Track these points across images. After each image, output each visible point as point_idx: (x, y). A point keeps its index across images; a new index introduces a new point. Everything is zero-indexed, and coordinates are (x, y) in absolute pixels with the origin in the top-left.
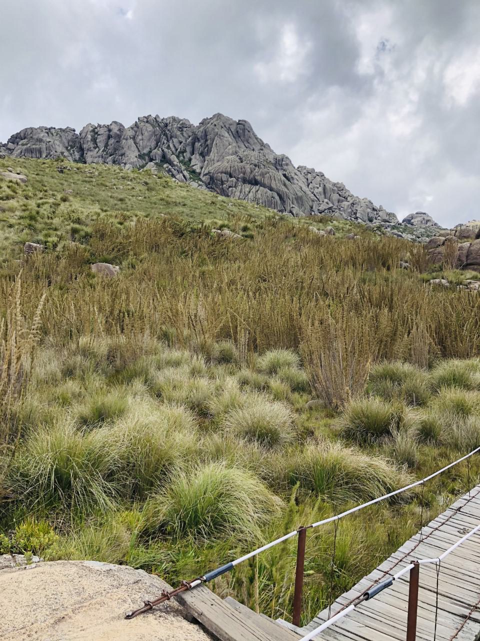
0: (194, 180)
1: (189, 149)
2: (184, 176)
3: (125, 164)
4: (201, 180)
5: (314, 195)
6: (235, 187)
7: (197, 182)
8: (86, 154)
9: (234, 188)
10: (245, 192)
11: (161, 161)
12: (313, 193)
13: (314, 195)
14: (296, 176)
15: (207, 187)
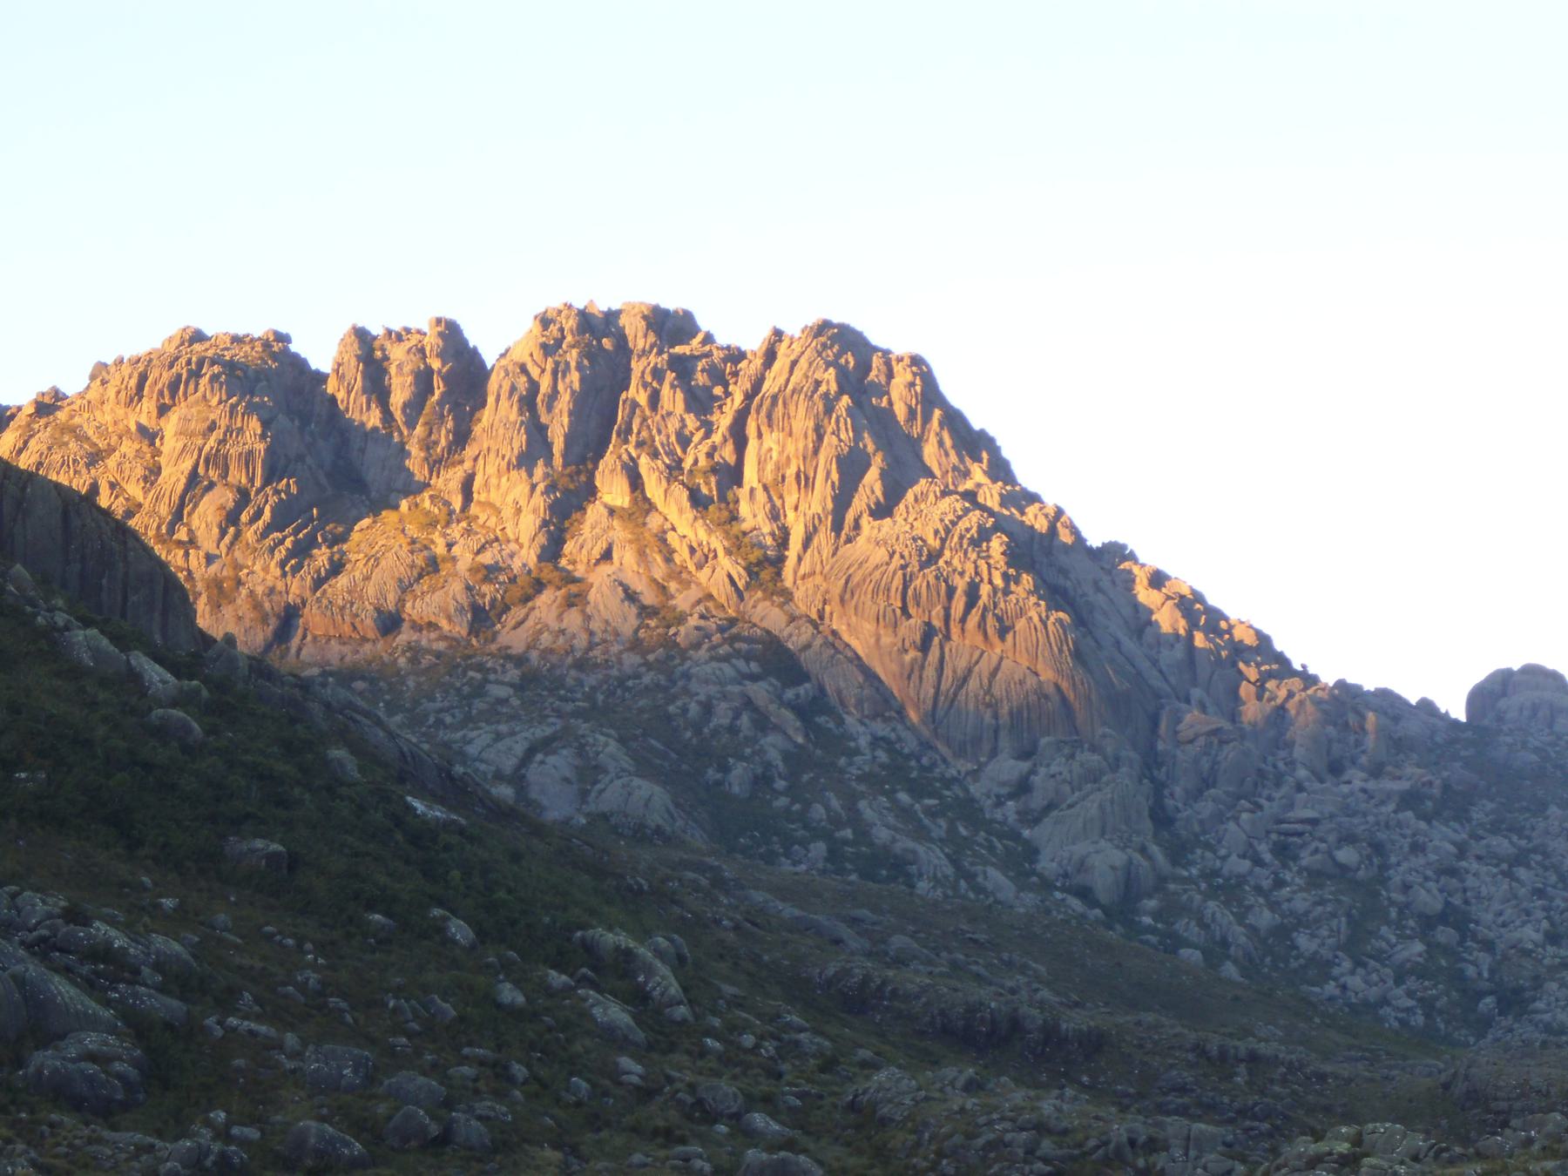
0: (769, 595)
1: (728, 454)
2: (730, 576)
3: (519, 511)
4: (788, 596)
5: (1161, 672)
6: (925, 647)
7: (781, 606)
8: (363, 451)
9: (920, 654)
10: (954, 672)
11: (634, 501)
12: (1155, 663)
13: (1161, 672)
14: (1100, 598)
15: (816, 626)
